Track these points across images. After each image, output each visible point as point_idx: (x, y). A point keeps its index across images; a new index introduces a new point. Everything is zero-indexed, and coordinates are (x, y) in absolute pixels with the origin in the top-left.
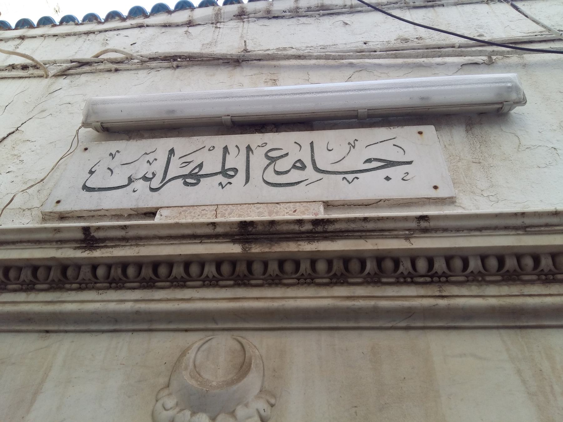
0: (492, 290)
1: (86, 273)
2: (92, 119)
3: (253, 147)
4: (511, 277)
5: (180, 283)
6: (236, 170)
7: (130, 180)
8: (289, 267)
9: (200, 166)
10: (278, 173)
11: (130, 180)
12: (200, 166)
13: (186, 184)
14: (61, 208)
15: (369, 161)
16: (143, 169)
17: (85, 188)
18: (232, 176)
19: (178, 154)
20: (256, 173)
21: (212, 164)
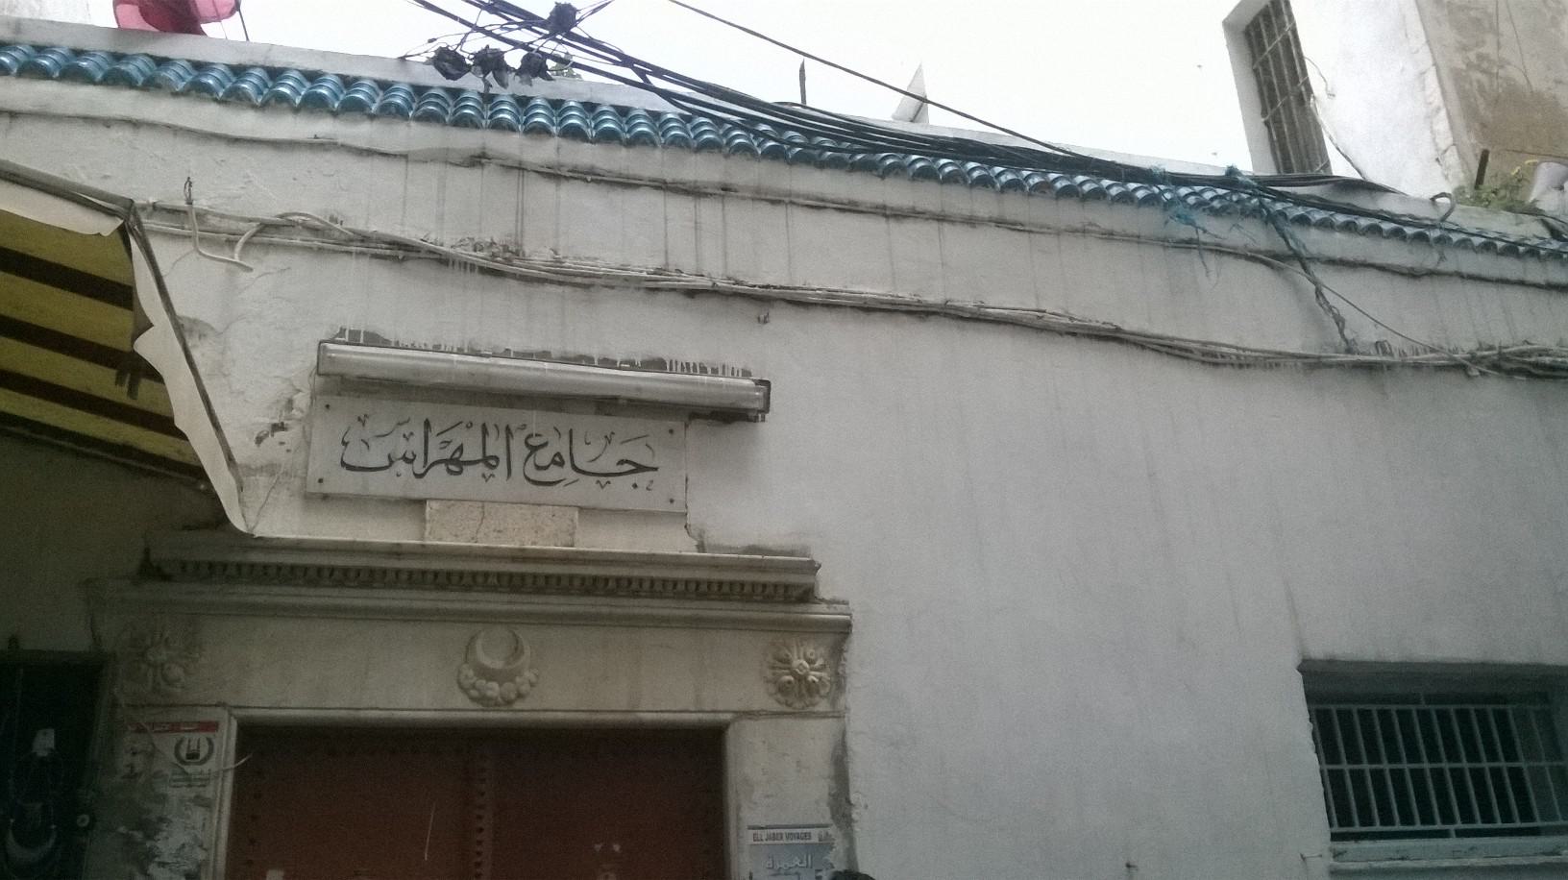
0: (688, 604)
1: (391, 576)
2: (331, 369)
3: (513, 428)
4: (702, 596)
5: (468, 588)
6: (496, 458)
7: (391, 462)
8: (554, 581)
9: (460, 449)
10: (538, 468)
11: (391, 462)
12: (460, 449)
13: (450, 471)
14: (326, 488)
15: (621, 462)
16: (402, 447)
17: (343, 464)
18: (493, 467)
19: (436, 429)
20: (517, 465)
21: (472, 452)
